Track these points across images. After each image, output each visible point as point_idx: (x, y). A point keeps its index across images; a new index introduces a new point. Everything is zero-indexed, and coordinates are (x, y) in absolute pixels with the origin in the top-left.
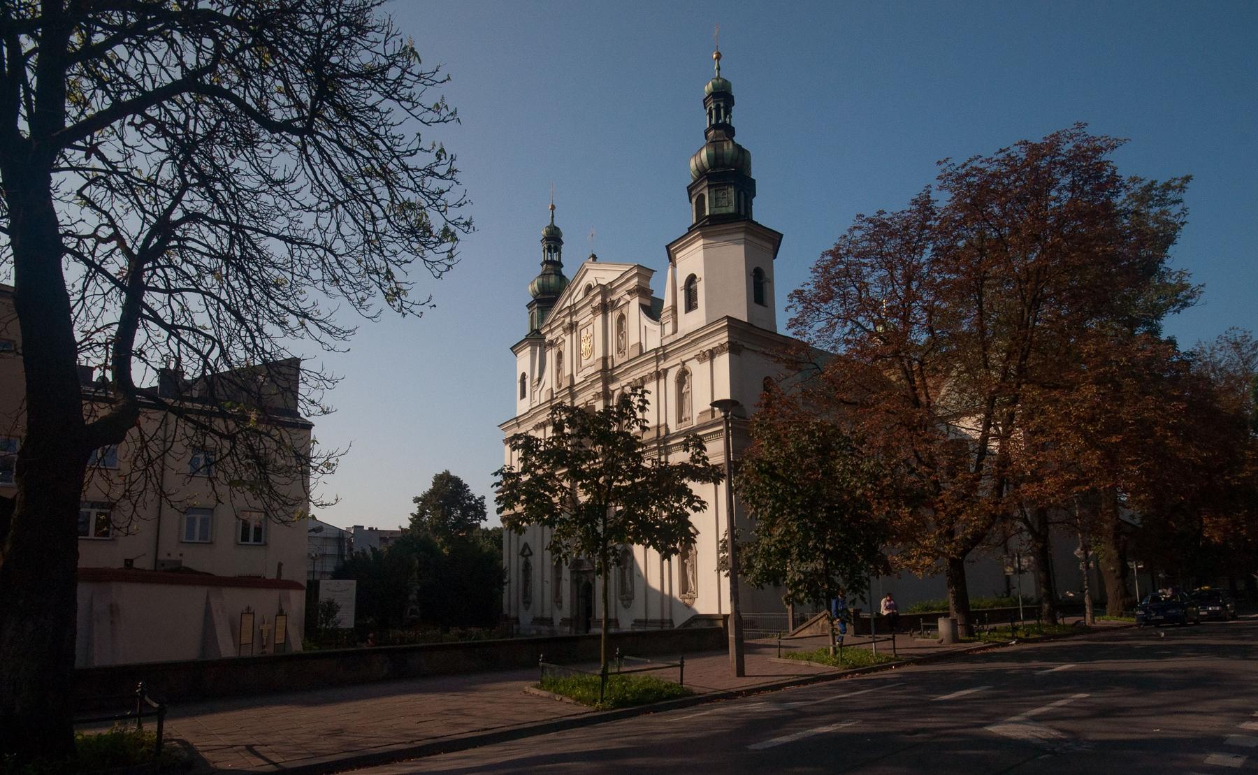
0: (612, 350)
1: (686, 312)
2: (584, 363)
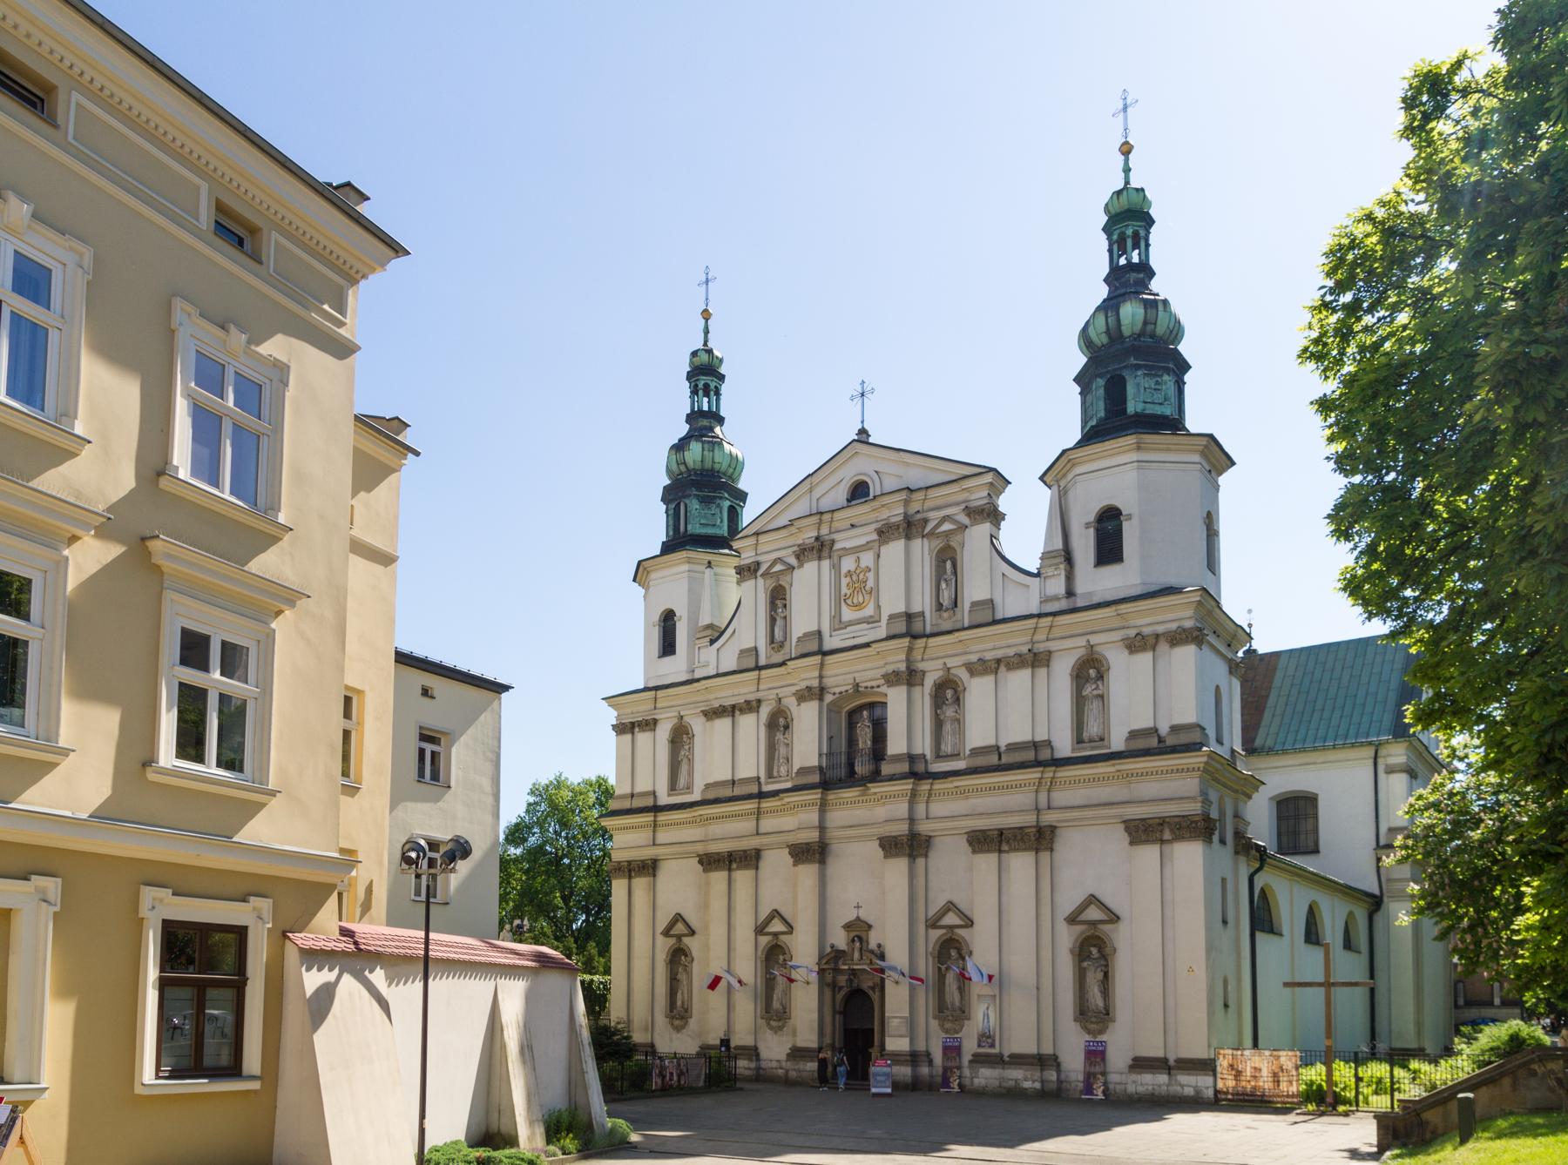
0: (922, 602)
2: (848, 614)
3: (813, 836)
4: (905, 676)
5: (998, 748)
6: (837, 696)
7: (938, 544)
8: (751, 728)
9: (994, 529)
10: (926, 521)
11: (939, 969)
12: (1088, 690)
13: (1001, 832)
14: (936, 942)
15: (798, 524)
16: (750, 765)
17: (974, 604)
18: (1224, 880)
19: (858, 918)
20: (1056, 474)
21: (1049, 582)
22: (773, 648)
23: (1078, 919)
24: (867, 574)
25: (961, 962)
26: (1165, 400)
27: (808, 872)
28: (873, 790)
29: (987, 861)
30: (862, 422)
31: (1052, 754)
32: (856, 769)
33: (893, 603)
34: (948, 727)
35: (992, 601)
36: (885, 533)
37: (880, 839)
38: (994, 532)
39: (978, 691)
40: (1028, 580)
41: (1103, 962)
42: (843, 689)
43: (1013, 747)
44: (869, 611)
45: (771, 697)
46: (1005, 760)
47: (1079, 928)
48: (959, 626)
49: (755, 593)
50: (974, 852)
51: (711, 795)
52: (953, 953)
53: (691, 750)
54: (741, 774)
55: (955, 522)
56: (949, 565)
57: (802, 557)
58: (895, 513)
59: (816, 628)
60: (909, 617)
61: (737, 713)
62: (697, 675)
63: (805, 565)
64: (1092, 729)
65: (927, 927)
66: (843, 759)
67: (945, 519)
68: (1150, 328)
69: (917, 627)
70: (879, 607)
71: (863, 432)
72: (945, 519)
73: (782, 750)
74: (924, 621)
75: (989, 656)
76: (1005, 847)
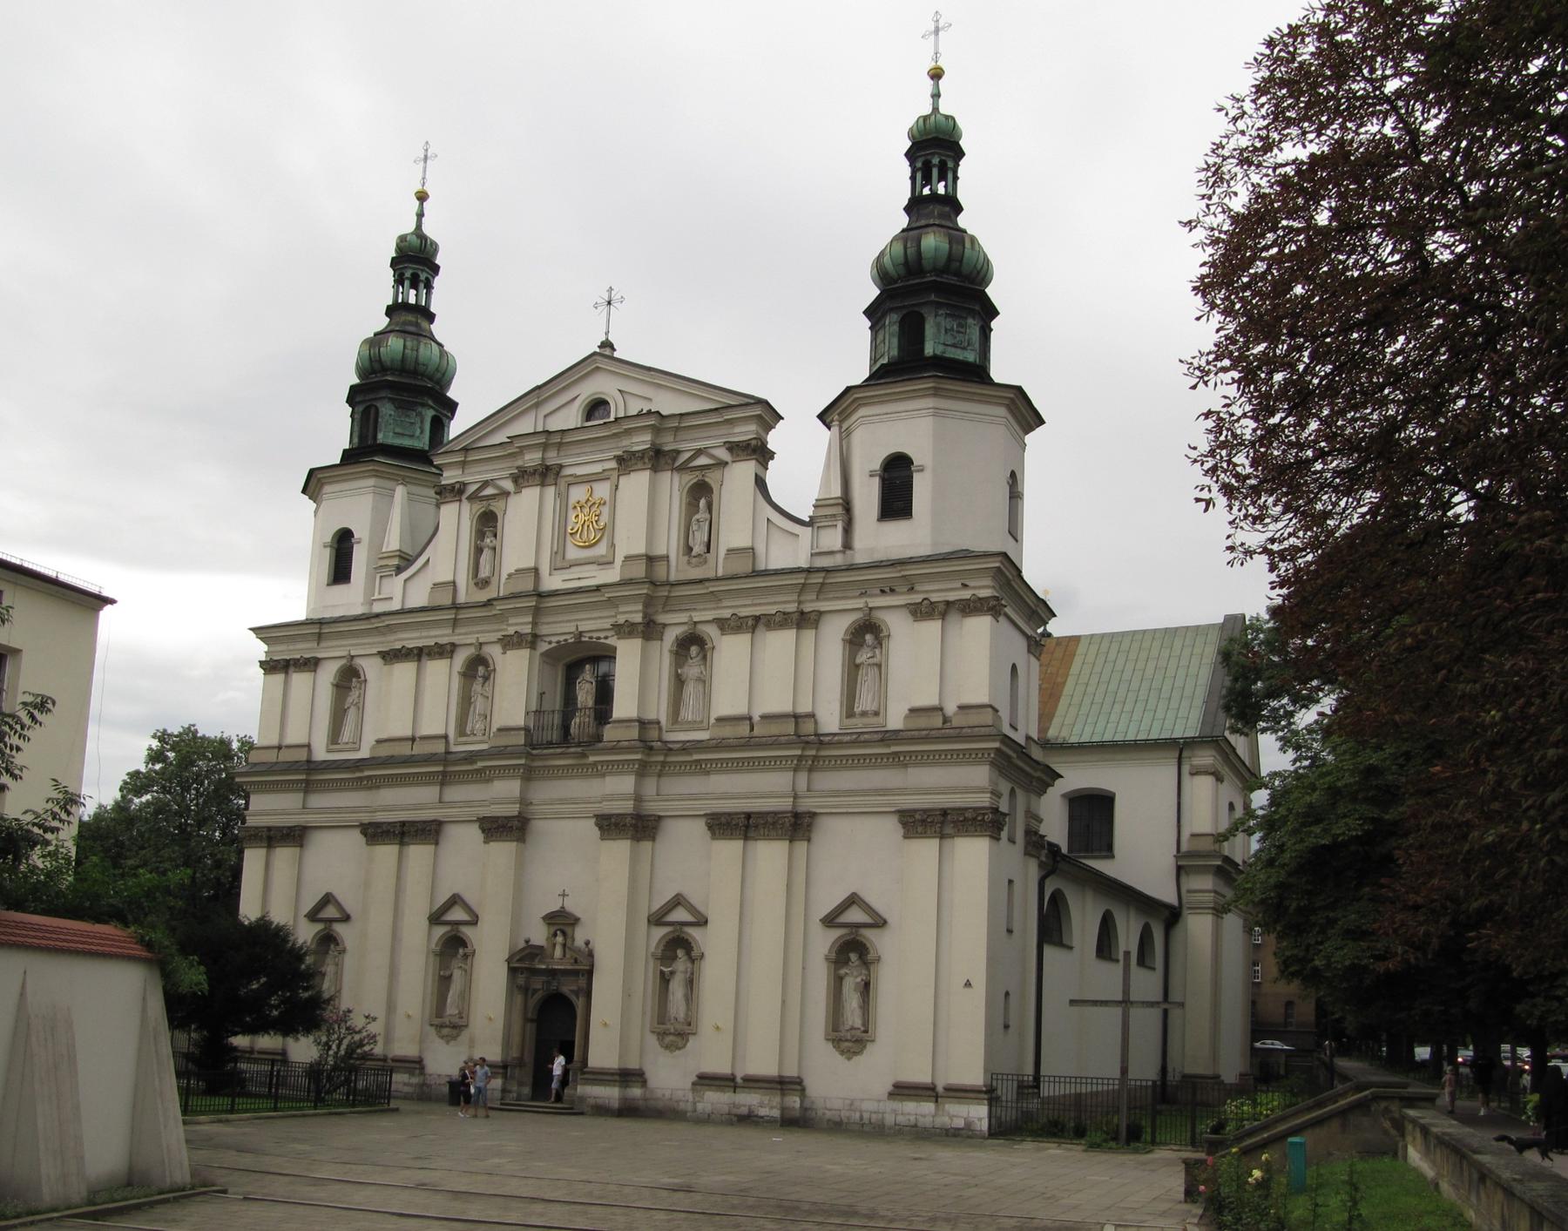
0: (669, 543)
1: (878, 520)
2: (573, 553)
3: (513, 810)
4: (640, 628)
5: (750, 719)
6: (554, 645)
7: (690, 479)
8: (441, 676)
9: (760, 471)
10: (678, 452)
11: (662, 973)
12: (863, 657)
13: (748, 816)
14: (660, 941)
16: (437, 719)
17: (730, 551)
18: (1010, 882)
19: (563, 907)
20: (835, 413)
21: (823, 533)
22: (476, 584)
24: (601, 508)
25: (689, 965)
26: (969, 345)
27: (503, 851)
28: (592, 759)
29: (731, 848)
30: (607, 333)
31: (816, 729)
32: (572, 731)
33: (631, 540)
34: (690, 689)
35: (753, 549)
36: (626, 462)
37: (596, 816)
38: (760, 471)
39: (730, 651)
40: (796, 528)
41: (864, 972)
42: (562, 638)
43: (766, 717)
44: (601, 550)
45: (468, 642)
46: (756, 732)
47: (837, 933)
48: (711, 575)
49: (455, 520)
50: (714, 836)
51: (385, 751)
52: (680, 953)
53: (362, 696)
54: (426, 730)
55: (712, 456)
56: (702, 502)
57: (521, 481)
58: (641, 442)
59: (532, 565)
60: (651, 560)
61: (424, 658)
62: (378, 608)
63: (523, 490)
64: (865, 702)
65: (649, 921)
66: (557, 719)
67: (699, 452)
68: (955, 265)
69: (660, 572)
70: (613, 545)
71: (607, 344)
72: (699, 452)
73: (479, 704)
75: (744, 612)
76: (751, 834)
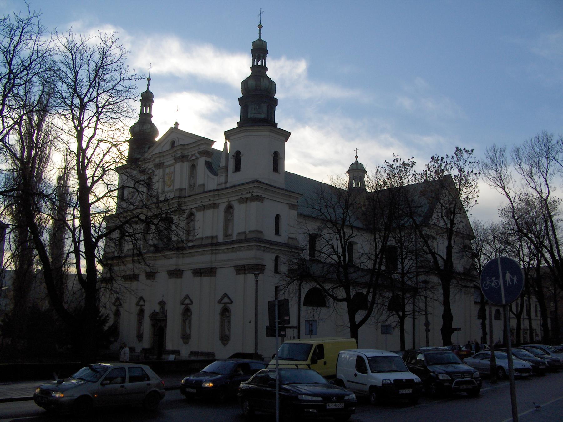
0: (185, 185)
2: (166, 189)
10: (188, 156)
15: (154, 157)
23: (222, 302)
50: (194, 277)
55: (196, 156)
60: (181, 190)
64: (230, 232)
67: (193, 155)
74: (186, 192)
